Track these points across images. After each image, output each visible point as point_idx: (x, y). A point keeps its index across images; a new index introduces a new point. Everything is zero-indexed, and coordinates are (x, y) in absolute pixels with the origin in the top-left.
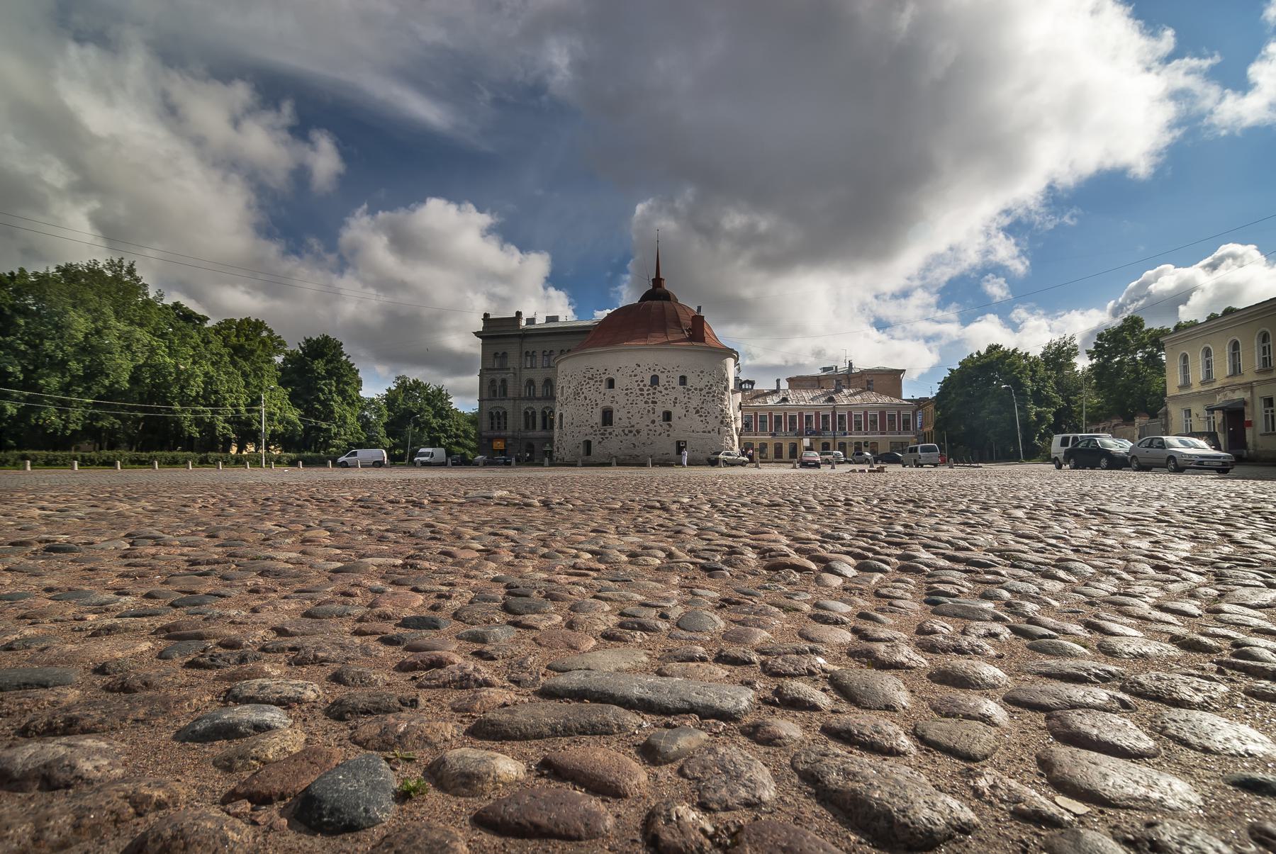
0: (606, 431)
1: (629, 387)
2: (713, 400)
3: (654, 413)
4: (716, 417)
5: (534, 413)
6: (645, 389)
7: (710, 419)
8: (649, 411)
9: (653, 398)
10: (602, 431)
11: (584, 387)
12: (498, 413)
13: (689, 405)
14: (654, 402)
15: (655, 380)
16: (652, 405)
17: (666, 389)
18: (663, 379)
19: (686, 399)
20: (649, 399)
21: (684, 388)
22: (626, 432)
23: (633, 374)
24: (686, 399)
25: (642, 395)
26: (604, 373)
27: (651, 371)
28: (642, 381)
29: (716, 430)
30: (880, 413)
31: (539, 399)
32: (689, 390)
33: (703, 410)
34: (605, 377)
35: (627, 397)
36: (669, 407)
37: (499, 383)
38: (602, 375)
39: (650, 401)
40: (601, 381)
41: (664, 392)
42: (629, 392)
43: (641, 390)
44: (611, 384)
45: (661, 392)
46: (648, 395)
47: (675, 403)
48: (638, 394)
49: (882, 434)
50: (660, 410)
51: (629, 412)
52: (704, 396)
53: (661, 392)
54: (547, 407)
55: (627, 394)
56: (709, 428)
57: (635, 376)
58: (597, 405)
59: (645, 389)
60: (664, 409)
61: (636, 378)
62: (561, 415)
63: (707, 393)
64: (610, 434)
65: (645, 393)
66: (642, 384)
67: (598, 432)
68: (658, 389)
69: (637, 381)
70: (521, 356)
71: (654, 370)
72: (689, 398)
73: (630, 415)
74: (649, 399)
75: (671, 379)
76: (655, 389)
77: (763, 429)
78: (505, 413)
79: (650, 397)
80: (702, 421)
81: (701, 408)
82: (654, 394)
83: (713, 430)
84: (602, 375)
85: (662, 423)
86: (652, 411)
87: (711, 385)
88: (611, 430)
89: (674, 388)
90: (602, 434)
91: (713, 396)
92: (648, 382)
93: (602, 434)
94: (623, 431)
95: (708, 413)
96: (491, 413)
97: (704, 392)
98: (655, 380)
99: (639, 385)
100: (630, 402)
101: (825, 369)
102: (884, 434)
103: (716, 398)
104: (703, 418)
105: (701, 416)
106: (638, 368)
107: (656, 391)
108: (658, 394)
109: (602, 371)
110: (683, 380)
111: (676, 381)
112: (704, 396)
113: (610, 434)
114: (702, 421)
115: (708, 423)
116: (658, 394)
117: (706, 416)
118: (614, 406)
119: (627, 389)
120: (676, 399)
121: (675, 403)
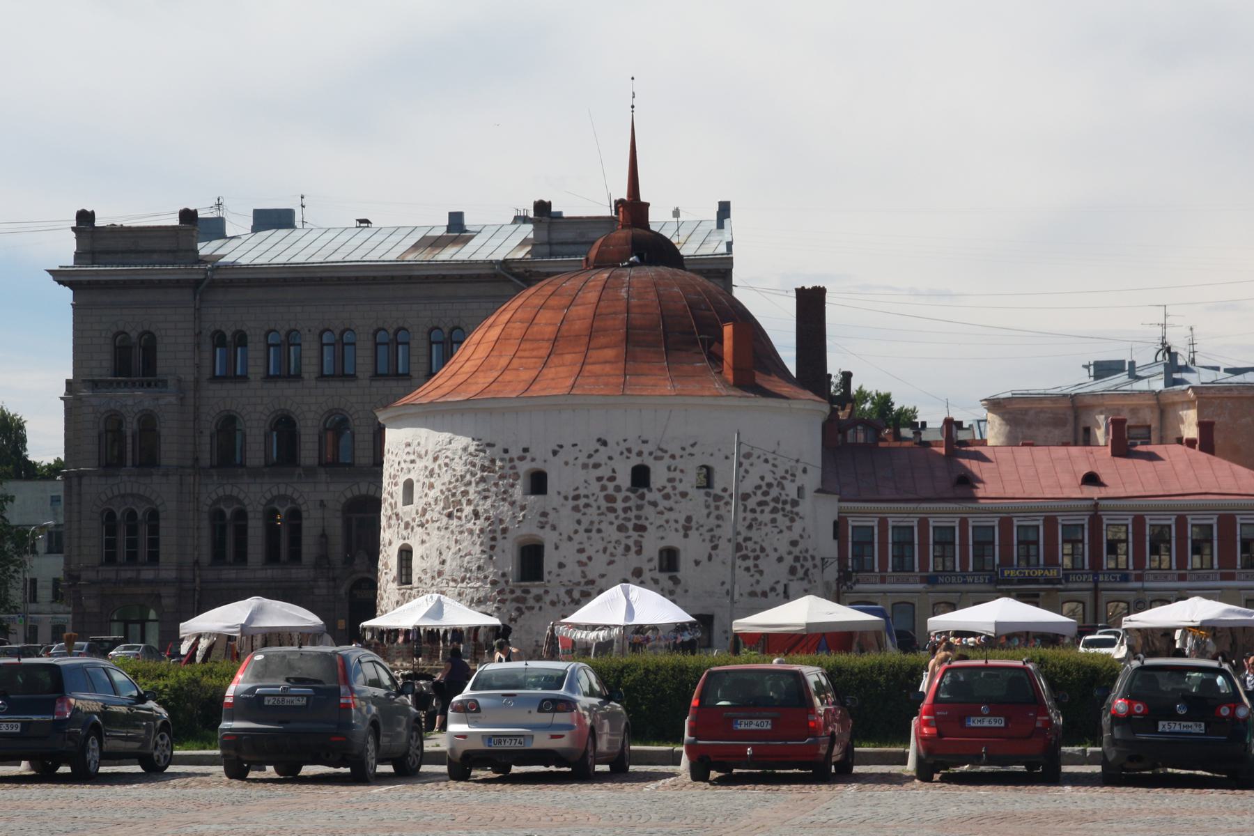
0: (527, 591)
1: (582, 492)
2: (774, 521)
3: (639, 552)
4: (780, 559)
5: (241, 515)
6: (620, 497)
7: (767, 564)
8: (627, 548)
9: (639, 518)
10: (518, 593)
11: (472, 489)
12: (132, 515)
13: (717, 532)
14: (640, 528)
15: (641, 476)
16: (635, 535)
17: (667, 497)
18: (658, 476)
19: (712, 521)
20: (629, 520)
21: (708, 494)
22: (576, 595)
23: (592, 461)
24: (712, 521)
25: (612, 510)
26: (521, 459)
27: (633, 455)
28: (612, 479)
29: (780, 588)
30: (1222, 519)
31: (255, 473)
32: (718, 498)
33: (750, 544)
34: (524, 467)
35: (578, 516)
36: (674, 540)
37: (131, 426)
38: (517, 463)
39: (630, 525)
40: (517, 477)
41: (663, 504)
42: (582, 502)
43: (611, 499)
44: (538, 483)
45: (655, 504)
46: (626, 510)
47: (687, 529)
48: (603, 509)
49: (1224, 577)
50: (652, 546)
51: (581, 551)
52: (753, 511)
53: (655, 504)
54: (283, 498)
55: (576, 509)
56: (765, 585)
57: (596, 466)
58: (504, 531)
59: (620, 497)
60: (664, 544)
61: (599, 472)
62: (405, 554)
63: (761, 504)
64: (538, 598)
65: (619, 505)
66: (611, 485)
67: (508, 596)
68: (650, 496)
69: (599, 479)
70: (198, 345)
71: (640, 454)
72: (719, 517)
73: (583, 557)
74: (629, 520)
75: (677, 475)
76: (642, 497)
77: (902, 565)
78: (154, 515)
79: (632, 514)
80: (747, 569)
81: (747, 539)
82: (639, 508)
83: (773, 589)
84: (517, 463)
85: (657, 575)
86: (634, 549)
87: (770, 485)
88: (541, 591)
89: (684, 495)
90: (517, 600)
91: (774, 510)
92: (625, 479)
93: (517, 600)
94: (569, 593)
95: (763, 549)
96: (111, 515)
97: (752, 503)
98: (641, 476)
99: (604, 488)
100: (585, 525)
101: (1103, 369)
102: (1231, 577)
103: (779, 516)
104: (750, 563)
105: (745, 558)
106: (602, 449)
107: (645, 502)
108: (649, 511)
109: (515, 452)
110: (708, 475)
111: (689, 481)
112: (753, 511)
113: (538, 598)
114: (747, 569)
115: (761, 572)
116: (649, 511)
117: (756, 558)
118: (548, 538)
119: (576, 498)
120: (689, 519)
121: (687, 529)
